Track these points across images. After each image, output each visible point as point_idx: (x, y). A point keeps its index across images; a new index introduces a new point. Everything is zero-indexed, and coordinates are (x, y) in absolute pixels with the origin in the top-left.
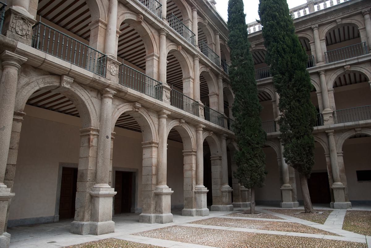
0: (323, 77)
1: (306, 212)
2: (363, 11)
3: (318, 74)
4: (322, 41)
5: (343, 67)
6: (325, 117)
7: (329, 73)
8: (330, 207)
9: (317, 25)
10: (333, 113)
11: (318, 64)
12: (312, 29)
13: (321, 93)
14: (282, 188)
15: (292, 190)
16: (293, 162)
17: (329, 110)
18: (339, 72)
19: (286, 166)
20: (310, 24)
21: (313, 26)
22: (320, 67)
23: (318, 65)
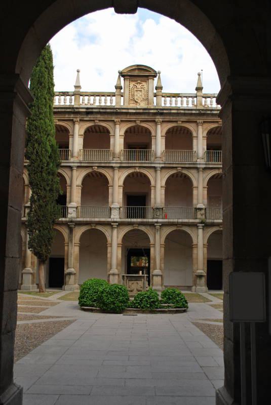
0: (75, 173)
1: (40, 292)
2: (116, 120)
3: (71, 168)
4: (80, 136)
5: (92, 167)
6: (70, 210)
7: (80, 170)
8: (62, 290)
9: (78, 119)
10: (77, 208)
11: (71, 159)
12: (74, 123)
13: (71, 186)
14: (24, 271)
15: (31, 273)
16: (35, 248)
17: (74, 204)
18: (89, 170)
19: (29, 252)
20: (72, 116)
21: (75, 119)
22: (73, 162)
23: (72, 160)
